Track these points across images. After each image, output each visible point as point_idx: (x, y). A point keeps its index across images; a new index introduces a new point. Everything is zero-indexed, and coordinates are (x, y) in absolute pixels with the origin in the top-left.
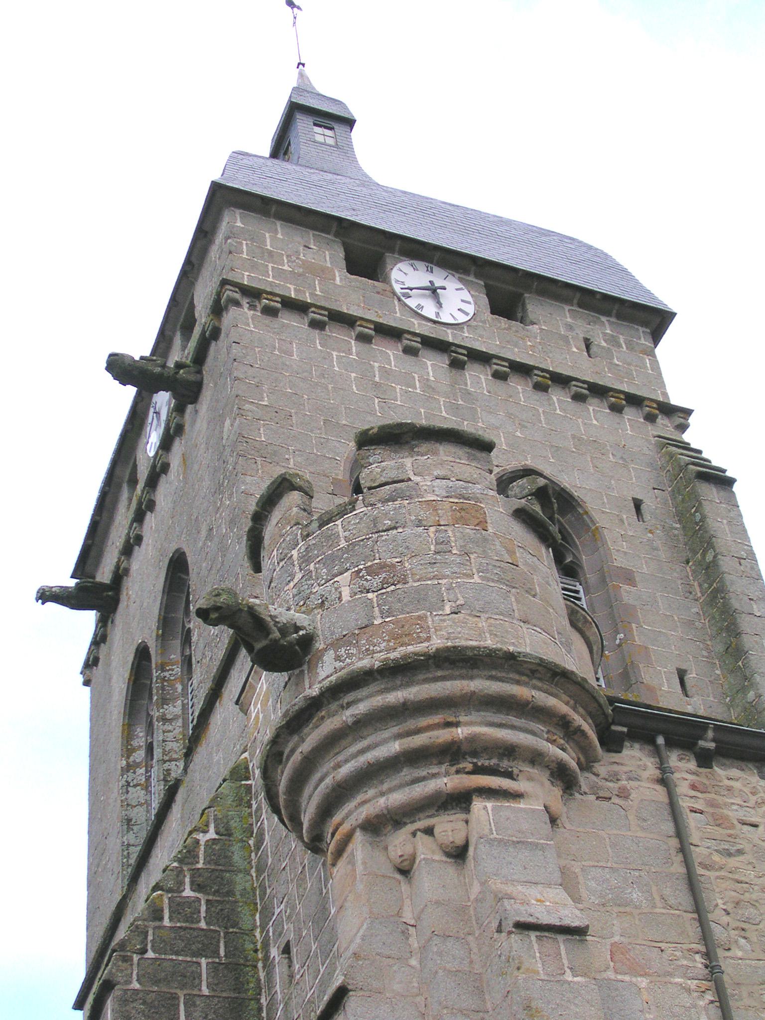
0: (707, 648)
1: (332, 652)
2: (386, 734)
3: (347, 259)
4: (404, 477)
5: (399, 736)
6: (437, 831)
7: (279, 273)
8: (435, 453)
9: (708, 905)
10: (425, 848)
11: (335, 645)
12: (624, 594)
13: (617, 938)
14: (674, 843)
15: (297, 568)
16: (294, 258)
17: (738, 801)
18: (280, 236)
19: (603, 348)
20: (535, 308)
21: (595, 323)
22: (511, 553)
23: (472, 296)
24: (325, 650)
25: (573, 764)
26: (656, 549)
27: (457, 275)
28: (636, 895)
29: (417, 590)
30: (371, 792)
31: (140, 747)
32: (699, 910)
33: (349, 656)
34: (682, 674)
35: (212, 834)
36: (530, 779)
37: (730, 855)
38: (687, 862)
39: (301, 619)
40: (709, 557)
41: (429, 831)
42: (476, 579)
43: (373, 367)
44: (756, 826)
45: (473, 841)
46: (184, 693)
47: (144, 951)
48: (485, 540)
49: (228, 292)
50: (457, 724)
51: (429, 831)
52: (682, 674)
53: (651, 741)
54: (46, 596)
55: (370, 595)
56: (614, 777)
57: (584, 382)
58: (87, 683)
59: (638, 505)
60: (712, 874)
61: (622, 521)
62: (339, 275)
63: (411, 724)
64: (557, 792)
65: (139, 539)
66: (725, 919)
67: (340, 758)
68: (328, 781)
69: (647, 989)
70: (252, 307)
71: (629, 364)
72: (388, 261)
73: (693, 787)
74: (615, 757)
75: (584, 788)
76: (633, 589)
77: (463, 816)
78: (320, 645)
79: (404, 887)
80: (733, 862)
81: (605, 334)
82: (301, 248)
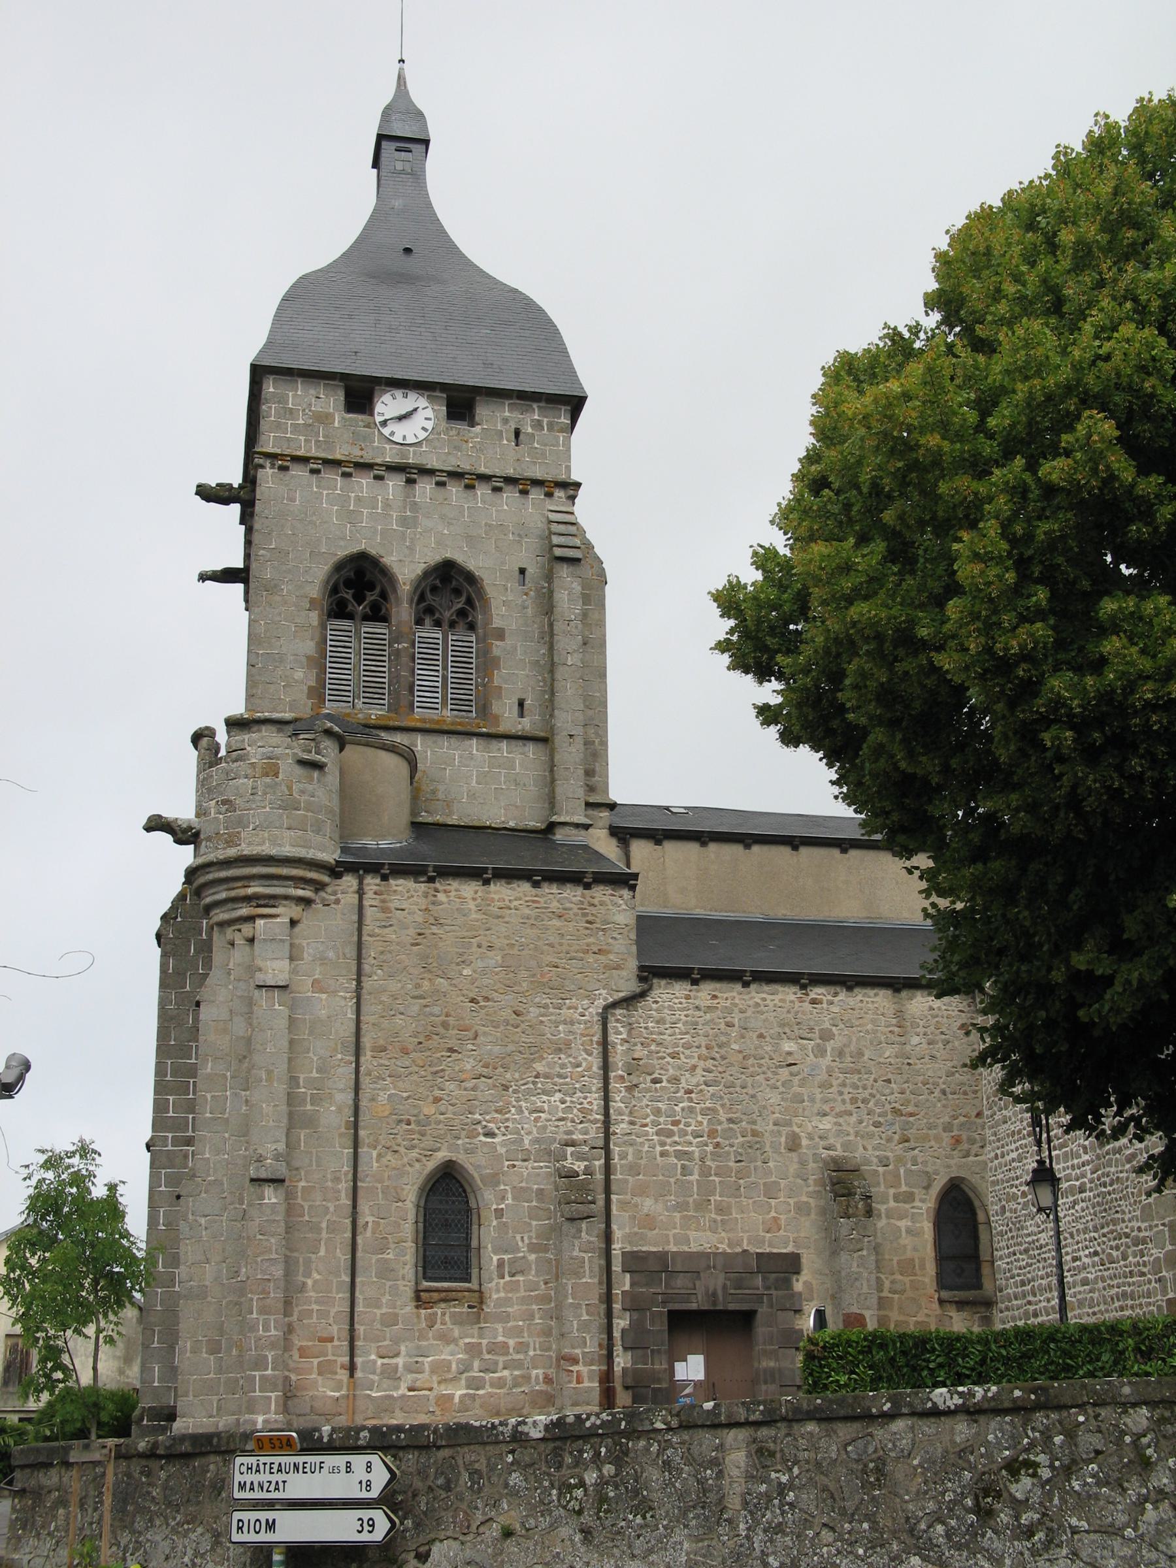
8: (259, 731)
10: (237, 935)
20: (482, 411)
21: (527, 411)
22: (290, 788)
26: (525, 608)
27: (427, 393)
28: (331, 954)
34: (521, 704)
37: (385, 927)
41: (239, 930)
52: (521, 704)
54: (203, 577)
56: (334, 893)
58: (247, 609)
59: (522, 571)
62: (339, 417)
66: (374, 961)
71: (546, 445)
72: (376, 394)
73: (375, 893)
74: (338, 881)
78: (202, 836)
80: (387, 930)
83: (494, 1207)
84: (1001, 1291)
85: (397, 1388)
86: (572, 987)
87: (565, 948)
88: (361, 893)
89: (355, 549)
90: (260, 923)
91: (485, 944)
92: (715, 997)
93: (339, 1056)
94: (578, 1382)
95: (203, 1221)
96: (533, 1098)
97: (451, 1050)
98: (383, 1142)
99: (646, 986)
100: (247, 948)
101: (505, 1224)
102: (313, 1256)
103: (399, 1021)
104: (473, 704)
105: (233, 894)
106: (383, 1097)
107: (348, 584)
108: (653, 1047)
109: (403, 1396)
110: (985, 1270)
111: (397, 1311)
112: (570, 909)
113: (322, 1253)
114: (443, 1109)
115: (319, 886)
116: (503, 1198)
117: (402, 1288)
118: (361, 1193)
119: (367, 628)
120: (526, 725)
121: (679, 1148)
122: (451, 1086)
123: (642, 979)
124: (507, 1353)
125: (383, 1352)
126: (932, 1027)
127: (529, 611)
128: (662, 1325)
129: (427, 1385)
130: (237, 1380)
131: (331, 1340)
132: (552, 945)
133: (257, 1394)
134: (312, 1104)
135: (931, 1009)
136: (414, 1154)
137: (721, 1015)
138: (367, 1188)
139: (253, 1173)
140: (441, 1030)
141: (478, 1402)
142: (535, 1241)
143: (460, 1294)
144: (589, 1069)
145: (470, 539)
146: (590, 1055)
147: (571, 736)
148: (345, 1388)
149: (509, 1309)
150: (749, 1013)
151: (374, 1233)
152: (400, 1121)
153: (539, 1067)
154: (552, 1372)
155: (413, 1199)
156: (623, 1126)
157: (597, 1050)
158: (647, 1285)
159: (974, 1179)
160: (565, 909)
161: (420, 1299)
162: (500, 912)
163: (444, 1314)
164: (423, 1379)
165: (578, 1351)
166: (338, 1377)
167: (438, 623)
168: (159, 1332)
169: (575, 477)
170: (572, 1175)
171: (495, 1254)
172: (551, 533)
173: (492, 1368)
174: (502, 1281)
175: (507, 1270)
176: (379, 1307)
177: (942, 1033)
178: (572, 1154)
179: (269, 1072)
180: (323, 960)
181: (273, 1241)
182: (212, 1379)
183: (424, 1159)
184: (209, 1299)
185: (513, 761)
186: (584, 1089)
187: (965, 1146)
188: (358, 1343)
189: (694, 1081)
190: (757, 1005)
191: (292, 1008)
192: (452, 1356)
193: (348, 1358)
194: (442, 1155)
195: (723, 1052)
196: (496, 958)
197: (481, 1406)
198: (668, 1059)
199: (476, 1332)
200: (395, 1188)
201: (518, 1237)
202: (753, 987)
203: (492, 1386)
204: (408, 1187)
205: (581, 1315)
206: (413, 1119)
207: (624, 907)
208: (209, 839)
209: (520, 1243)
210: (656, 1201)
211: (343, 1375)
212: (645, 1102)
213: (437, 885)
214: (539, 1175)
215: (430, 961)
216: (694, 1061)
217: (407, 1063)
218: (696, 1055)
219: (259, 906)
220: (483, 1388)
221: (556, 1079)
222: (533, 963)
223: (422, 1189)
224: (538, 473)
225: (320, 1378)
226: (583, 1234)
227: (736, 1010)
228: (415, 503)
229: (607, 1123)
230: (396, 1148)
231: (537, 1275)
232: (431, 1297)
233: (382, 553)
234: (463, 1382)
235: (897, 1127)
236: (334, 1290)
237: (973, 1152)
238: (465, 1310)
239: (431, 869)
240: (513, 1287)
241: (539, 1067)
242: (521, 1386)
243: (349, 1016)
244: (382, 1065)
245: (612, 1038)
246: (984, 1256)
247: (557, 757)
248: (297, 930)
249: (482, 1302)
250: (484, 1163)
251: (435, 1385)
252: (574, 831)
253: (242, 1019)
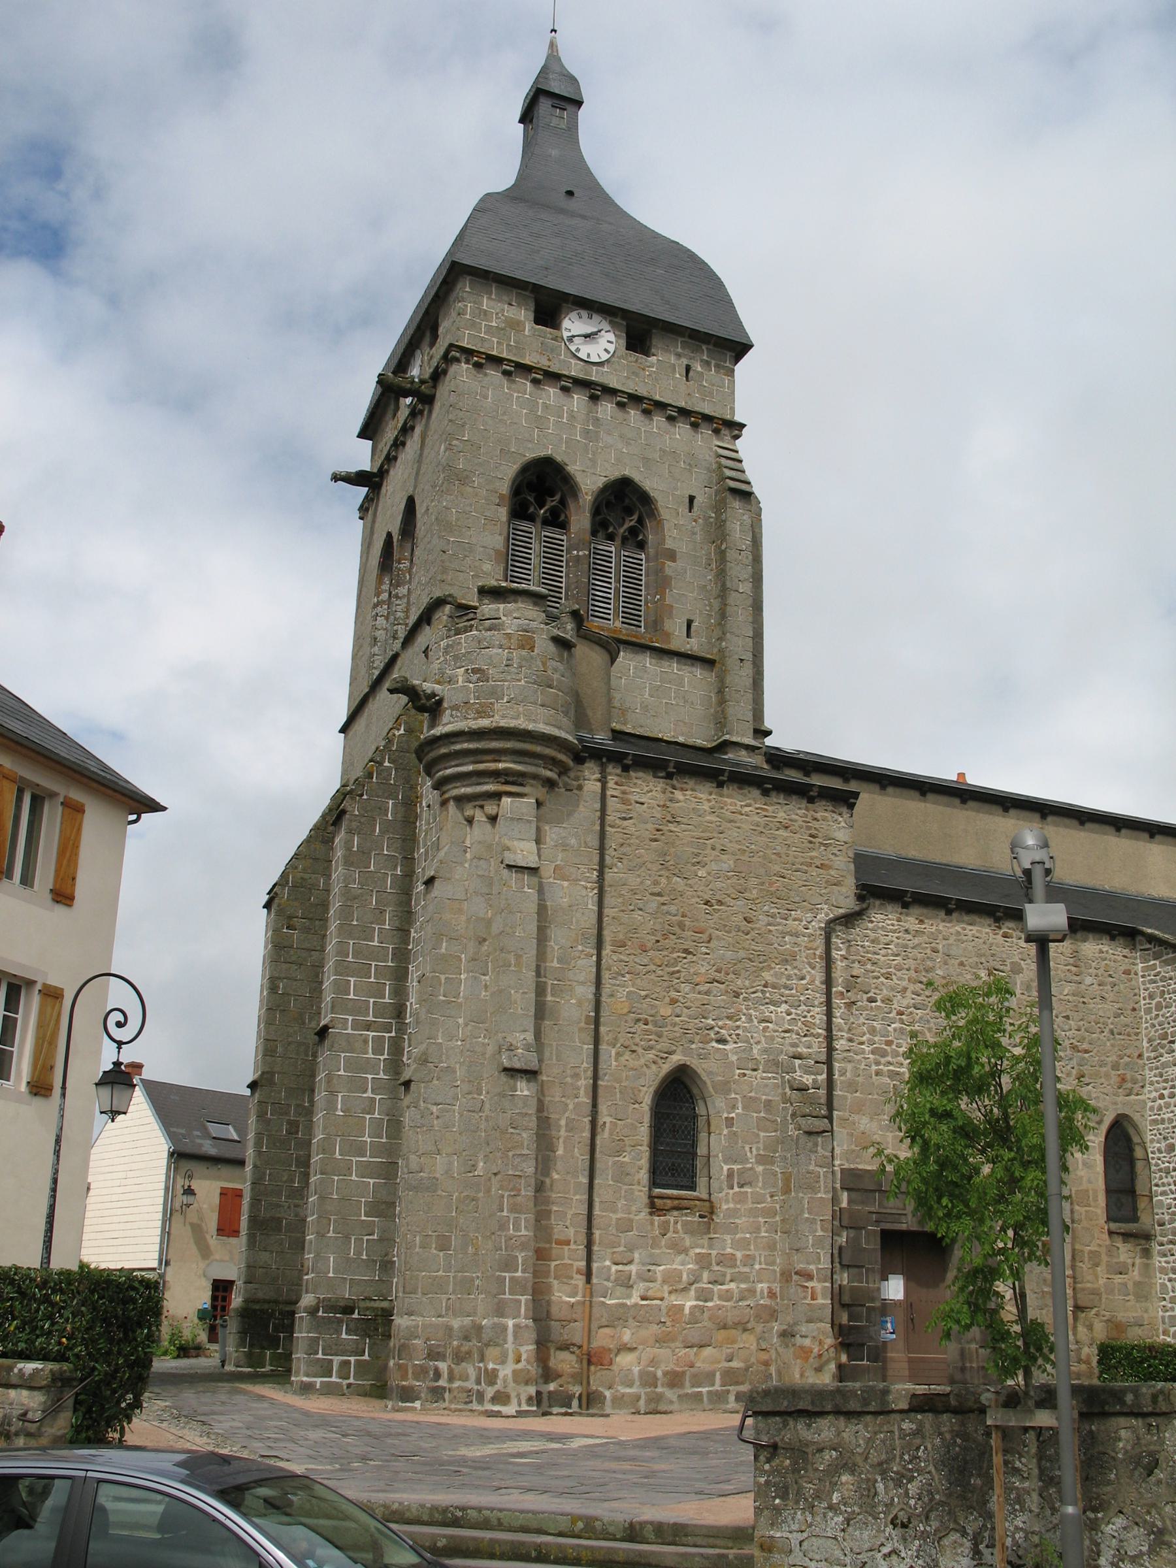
0: (710, 605)
2: (467, 760)
4: (497, 616)
6: (486, 808)
7: (489, 328)
8: (516, 602)
9: (607, 846)
11: (453, 708)
12: (667, 568)
13: (558, 863)
14: (598, 814)
17: (638, 790)
18: (493, 297)
19: (698, 372)
20: (657, 342)
23: (616, 336)
24: (447, 709)
26: (695, 534)
27: (609, 318)
28: (573, 841)
30: (458, 784)
32: (602, 849)
33: (457, 717)
34: (689, 624)
35: (402, 731)
36: (532, 786)
37: (625, 819)
38: (602, 825)
39: (437, 688)
40: (723, 547)
41: (482, 807)
42: (523, 682)
43: (538, 403)
44: (643, 804)
45: (500, 815)
46: (410, 582)
48: (532, 657)
50: (500, 761)
51: (482, 807)
52: (689, 624)
53: (600, 759)
54: (336, 478)
55: (471, 685)
59: (692, 499)
60: (613, 830)
62: (529, 327)
63: (479, 757)
64: (544, 790)
66: (614, 853)
67: (448, 765)
69: (567, 887)
70: (467, 362)
71: (713, 385)
73: (616, 783)
74: (580, 767)
75: (561, 785)
76: (672, 564)
77: (497, 802)
78: (445, 705)
79: (468, 828)
80: (626, 823)
81: (702, 360)
83: (725, 1115)
84: (1162, 1224)
85: (629, 1297)
86: (797, 899)
87: (790, 859)
88: (603, 781)
89: (542, 454)
90: (506, 801)
91: (719, 847)
92: (921, 922)
93: (580, 948)
94: (813, 1299)
95: (434, 1109)
96: (763, 1008)
97: (686, 951)
98: (622, 1041)
99: (864, 906)
100: (489, 826)
101: (735, 1133)
102: (552, 1154)
103: (637, 915)
104: (642, 619)
105: (481, 766)
106: (622, 993)
107: (531, 487)
108: (869, 966)
109: (636, 1305)
110: (1142, 1204)
111: (631, 1216)
112: (796, 821)
113: (560, 1152)
114: (678, 1011)
115: (564, 770)
116: (734, 1107)
117: (637, 1193)
118: (601, 1092)
119: (548, 532)
120: (693, 645)
121: (891, 1068)
122: (686, 988)
123: (860, 898)
124: (734, 1266)
125: (618, 1258)
126: (1102, 970)
127: (698, 537)
128: (875, 1244)
129: (659, 1295)
130: (472, 1280)
131: (568, 1243)
132: (778, 854)
133: (507, 1296)
134: (552, 995)
135: (1101, 952)
136: (651, 1055)
137: (927, 940)
138: (606, 1086)
139: (507, 1064)
140: (676, 929)
141: (706, 1315)
142: (762, 1152)
143: (692, 1203)
144: (812, 982)
145: (646, 460)
146: (813, 968)
147: (742, 660)
148: (580, 1294)
149: (737, 1221)
150: (951, 941)
151: (611, 1134)
152: (638, 1020)
153: (767, 976)
154: (776, 1287)
155: (649, 1103)
156: (842, 1042)
157: (820, 964)
158: (863, 1203)
159: (1136, 1117)
160: (790, 820)
161: (654, 1207)
162: (732, 816)
163: (676, 1223)
164: (655, 1288)
165: (812, 1267)
166: (573, 1282)
167: (611, 537)
168: (335, 1221)
169: (738, 418)
170: (802, 1089)
171: (726, 1163)
172: (720, 466)
173: (720, 1279)
174: (731, 1192)
175: (736, 1181)
176: (614, 1212)
177: (1110, 976)
178: (799, 1066)
179: (518, 957)
180: (565, 847)
181: (524, 1135)
182: (441, 1277)
183: (660, 1061)
184: (440, 1192)
185: (681, 678)
186: (809, 1003)
187: (1129, 1085)
188: (595, 1248)
189: (905, 1002)
190: (958, 933)
191: (541, 891)
192: (685, 1266)
193: (584, 1263)
194: (677, 1059)
195: (930, 975)
196: (728, 862)
197: (710, 1319)
198: (882, 979)
199: (705, 1242)
200: (632, 1089)
201: (747, 1149)
202: (955, 915)
203: (720, 1298)
204: (645, 1089)
205: (816, 1231)
206: (650, 1019)
207: (843, 824)
208: (455, 708)
209: (749, 1154)
210: (872, 1119)
211: (580, 1281)
212: (862, 1020)
213: (675, 782)
214: (766, 1086)
215: (668, 858)
216: (905, 983)
217: (645, 961)
218: (906, 977)
219: (506, 783)
220: (712, 1300)
221: (782, 990)
222: (762, 871)
223: (656, 1092)
224: (707, 411)
225: (555, 1282)
226: (819, 1148)
227: (941, 937)
228: (598, 419)
229: (830, 1038)
230: (634, 1048)
231: (764, 1188)
232: (665, 1204)
233: (567, 461)
234: (692, 1293)
235: (1074, 1062)
236: (572, 1192)
237: (1135, 1091)
238: (697, 1219)
239: (672, 764)
240: (741, 1198)
241: (767, 976)
242: (746, 1300)
243: (590, 906)
244: (621, 961)
245: (836, 954)
246: (1140, 1189)
247: (728, 680)
248: (543, 809)
249: (712, 1213)
250: (715, 1070)
251: (666, 1295)
252: (744, 752)
253: (483, 899)
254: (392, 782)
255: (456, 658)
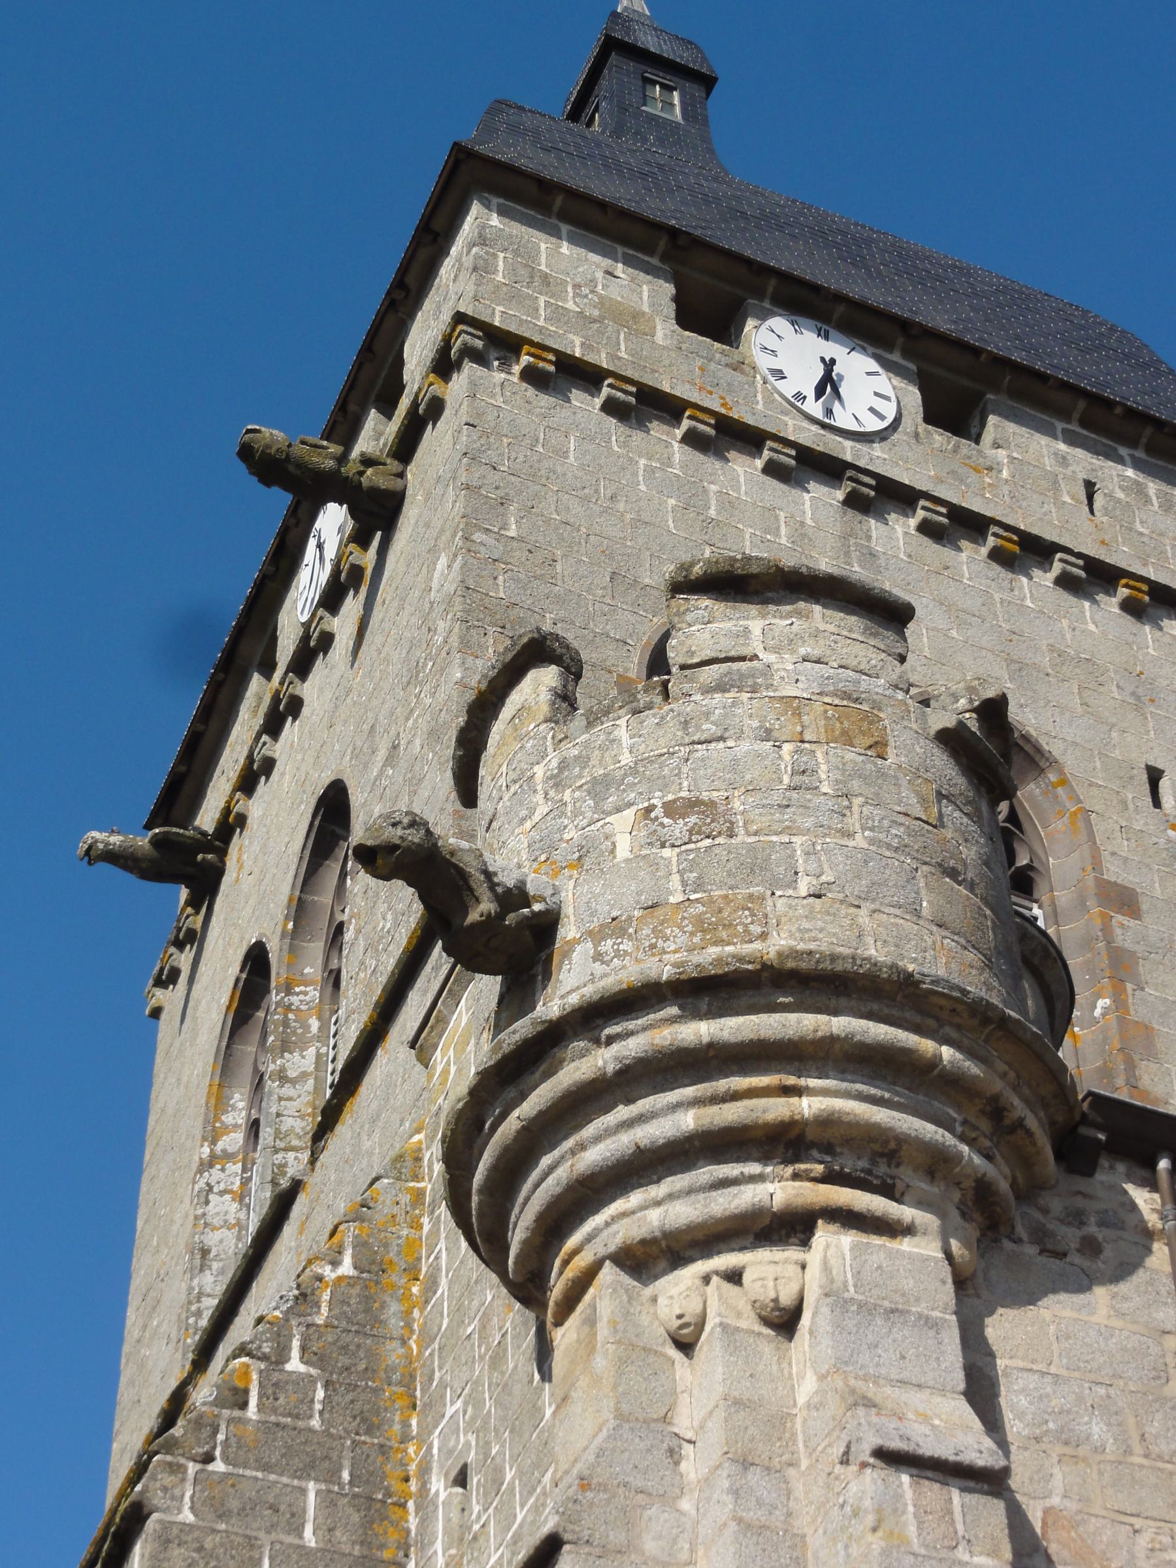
1: (590, 945)
3: (677, 299)
4: (746, 651)
5: (697, 1102)
6: (747, 1278)
7: (558, 314)
8: (807, 616)
11: (597, 936)
13: (1056, 1501)
15: (539, 797)
16: (585, 291)
19: (1119, 501)
23: (894, 388)
24: (577, 941)
25: (1004, 1186)
28: (1097, 1429)
29: (751, 848)
31: (236, 1126)
35: (347, 1267)
41: (734, 1277)
42: (859, 841)
43: (705, 490)
47: (208, 1458)
49: (464, 337)
51: (734, 1277)
55: (667, 852)
56: (1077, 1218)
57: (1079, 555)
61: (1124, 803)
65: (269, 765)
68: (562, 1174)
74: (1081, 1183)
75: (1021, 1231)
76: (1132, 923)
78: (568, 931)
82: (599, 275)
254: (315, 1423)
255: (599, 788)
